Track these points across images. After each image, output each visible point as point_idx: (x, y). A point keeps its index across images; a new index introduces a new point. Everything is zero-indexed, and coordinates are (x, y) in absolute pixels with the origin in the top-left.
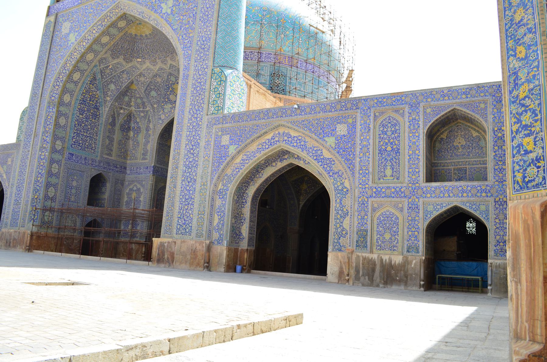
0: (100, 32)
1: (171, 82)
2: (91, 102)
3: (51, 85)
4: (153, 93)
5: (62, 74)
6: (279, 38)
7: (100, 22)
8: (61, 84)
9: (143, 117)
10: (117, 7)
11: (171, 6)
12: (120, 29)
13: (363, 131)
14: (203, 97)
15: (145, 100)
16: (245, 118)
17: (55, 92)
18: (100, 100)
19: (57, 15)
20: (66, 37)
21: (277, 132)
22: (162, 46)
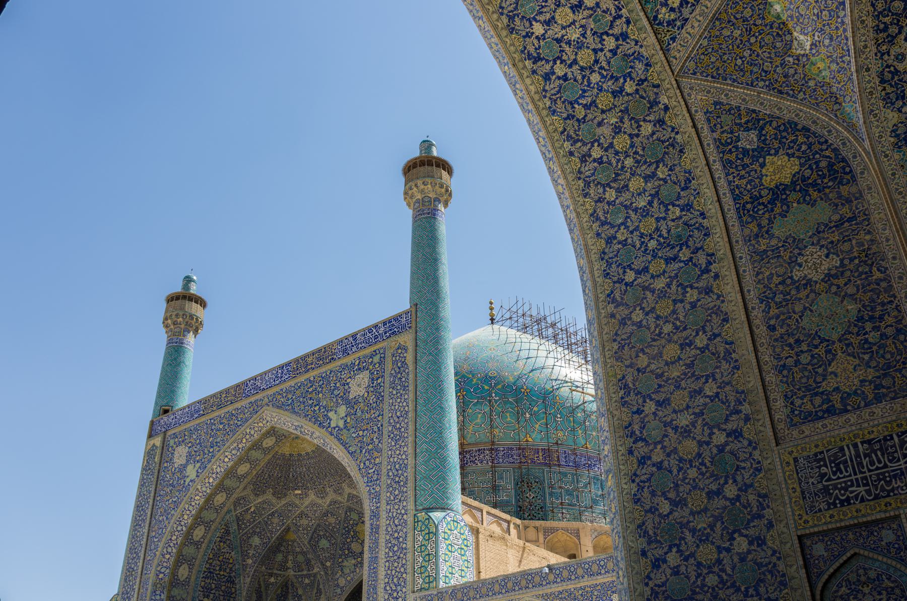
0: (236, 459)
1: (351, 522)
2: (222, 573)
4: (324, 543)
5: (177, 533)
6: (522, 419)
7: (235, 445)
8: (174, 551)
9: (307, 585)
11: (344, 415)
12: (266, 451)
14: (404, 562)
15: (310, 556)
17: (165, 564)
18: (237, 566)
20: (181, 471)
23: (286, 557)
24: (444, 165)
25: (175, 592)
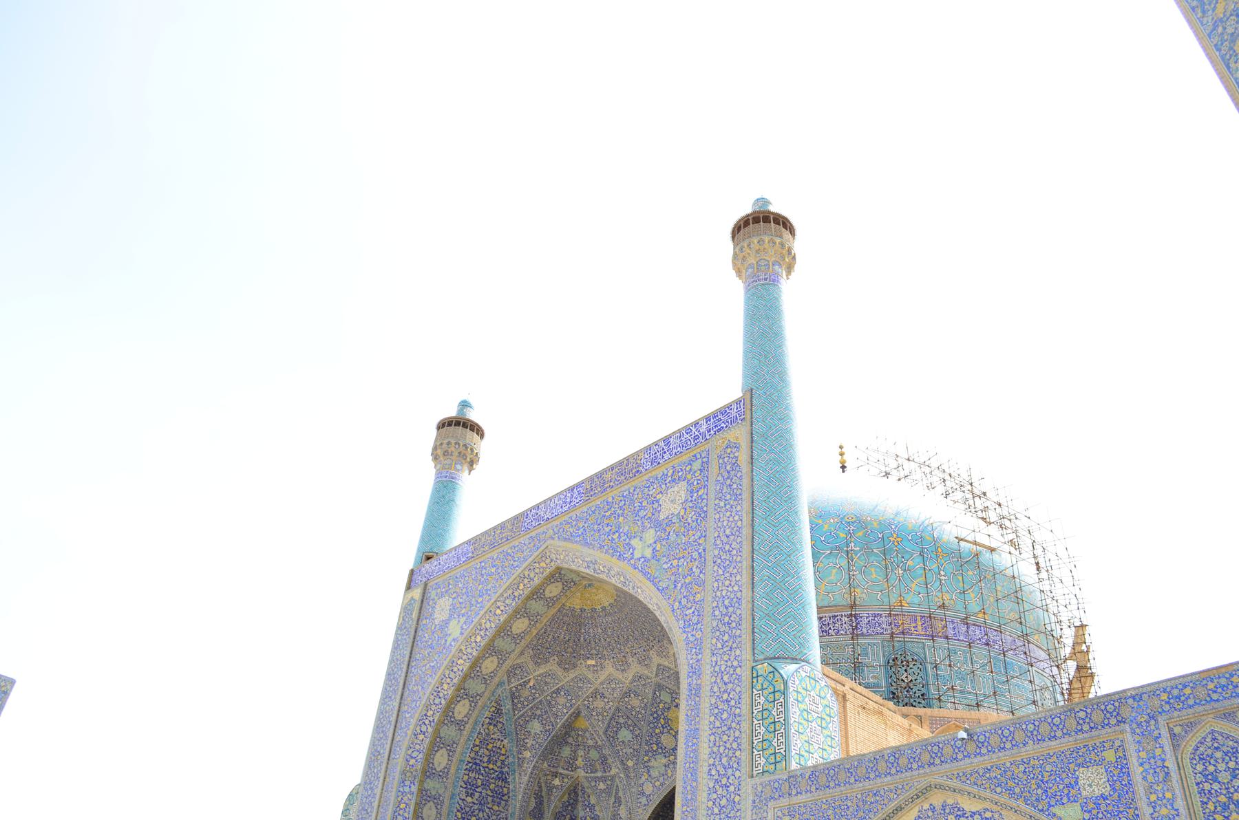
0: (510, 611)
1: (661, 705)
2: (491, 766)
3: (409, 732)
4: (624, 735)
5: (433, 707)
6: (893, 578)
7: (510, 592)
8: (430, 730)
10: (543, 556)
13: (1150, 778)
14: (737, 733)
15: (606, 752)
16: (842, 776)
17: (417, 747)
18: (511, 759)
19: (426, 585)
20: (442, 629)
21: (926, 806)
22: (638, 628)
23: (575, 752)
24: (783, 223)
25: (430, 784)
